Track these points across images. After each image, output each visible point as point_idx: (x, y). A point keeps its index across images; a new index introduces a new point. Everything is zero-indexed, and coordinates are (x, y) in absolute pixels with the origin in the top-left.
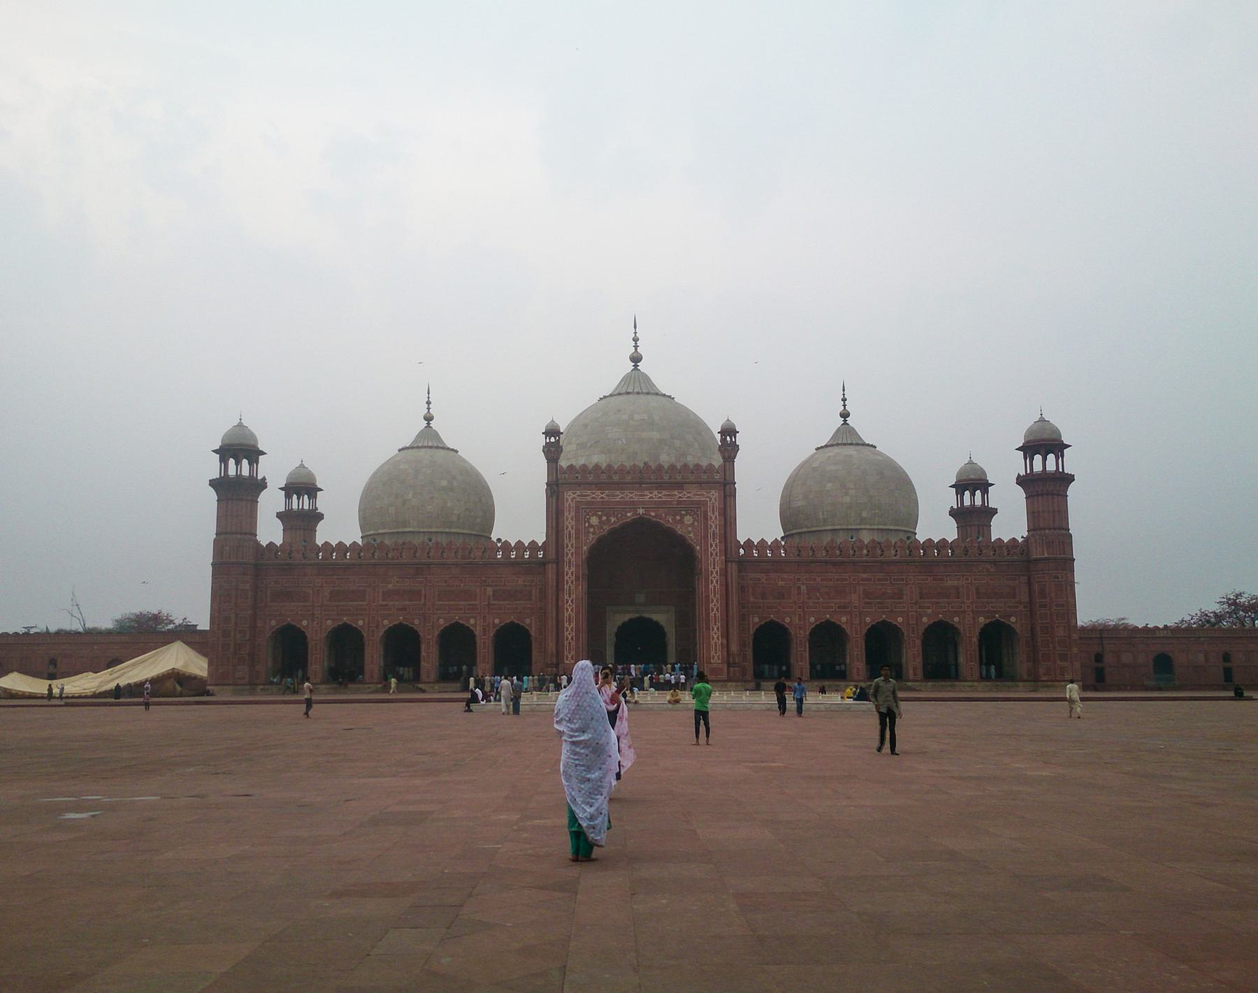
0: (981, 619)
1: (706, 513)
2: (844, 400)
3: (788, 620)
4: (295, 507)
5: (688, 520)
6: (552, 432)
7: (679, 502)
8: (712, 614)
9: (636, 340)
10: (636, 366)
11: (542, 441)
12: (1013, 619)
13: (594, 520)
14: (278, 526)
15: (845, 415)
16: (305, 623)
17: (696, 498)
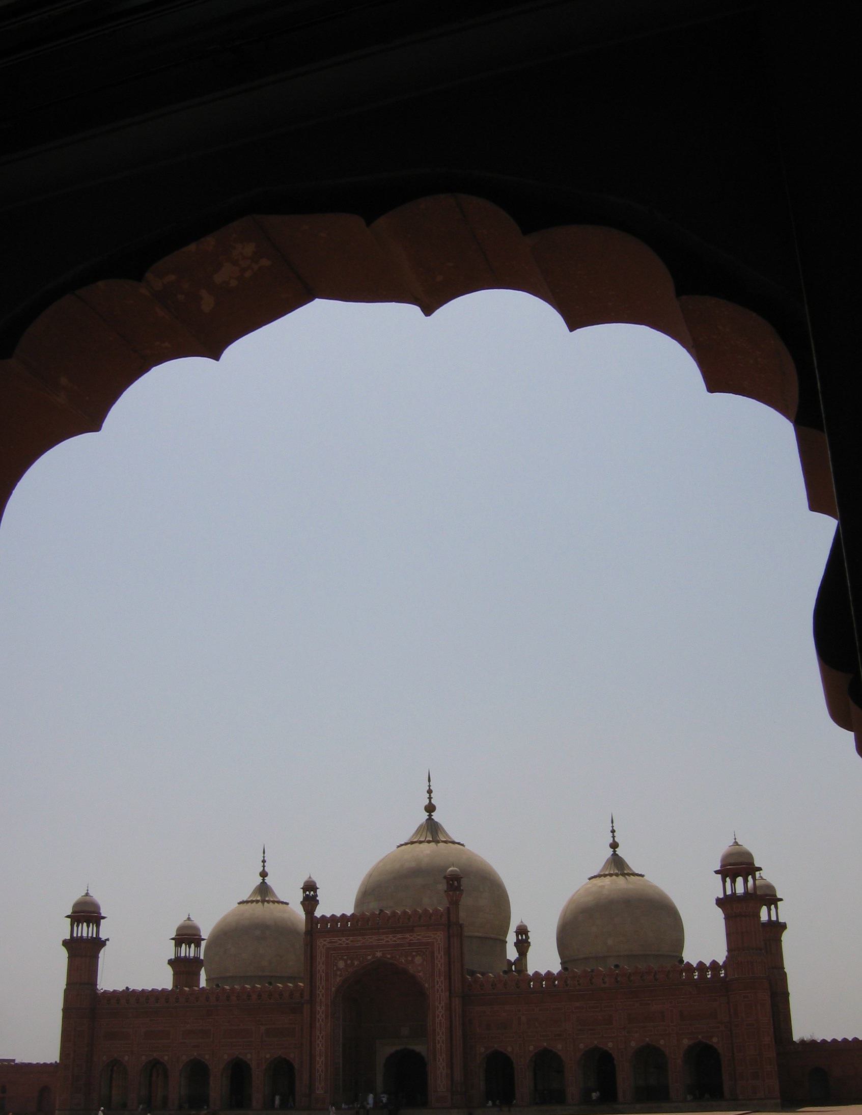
0: (686, 1042)
1: (433, 952)
2: (613, 831)
3: (509, 1049)
4: (183, 955)
5: (418, 960)
6: (310, 887)
7: (410, 944)
8: (438, 1046)
9: (430, 792)
10: (430, 816)
11: (300, 896)
12: (715, 1040)
13: (341, 964)
14: (169, 971)
15: (614, 845)
16: (126, 1058)
17: (424, 940)
